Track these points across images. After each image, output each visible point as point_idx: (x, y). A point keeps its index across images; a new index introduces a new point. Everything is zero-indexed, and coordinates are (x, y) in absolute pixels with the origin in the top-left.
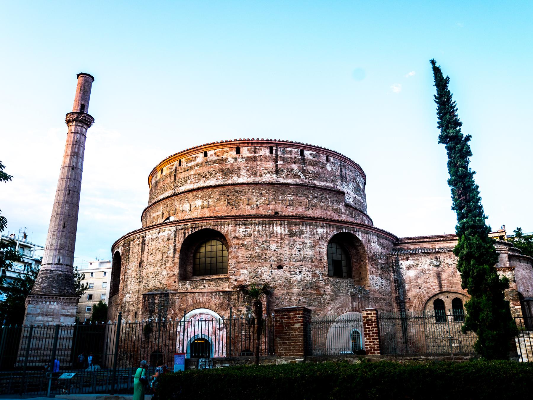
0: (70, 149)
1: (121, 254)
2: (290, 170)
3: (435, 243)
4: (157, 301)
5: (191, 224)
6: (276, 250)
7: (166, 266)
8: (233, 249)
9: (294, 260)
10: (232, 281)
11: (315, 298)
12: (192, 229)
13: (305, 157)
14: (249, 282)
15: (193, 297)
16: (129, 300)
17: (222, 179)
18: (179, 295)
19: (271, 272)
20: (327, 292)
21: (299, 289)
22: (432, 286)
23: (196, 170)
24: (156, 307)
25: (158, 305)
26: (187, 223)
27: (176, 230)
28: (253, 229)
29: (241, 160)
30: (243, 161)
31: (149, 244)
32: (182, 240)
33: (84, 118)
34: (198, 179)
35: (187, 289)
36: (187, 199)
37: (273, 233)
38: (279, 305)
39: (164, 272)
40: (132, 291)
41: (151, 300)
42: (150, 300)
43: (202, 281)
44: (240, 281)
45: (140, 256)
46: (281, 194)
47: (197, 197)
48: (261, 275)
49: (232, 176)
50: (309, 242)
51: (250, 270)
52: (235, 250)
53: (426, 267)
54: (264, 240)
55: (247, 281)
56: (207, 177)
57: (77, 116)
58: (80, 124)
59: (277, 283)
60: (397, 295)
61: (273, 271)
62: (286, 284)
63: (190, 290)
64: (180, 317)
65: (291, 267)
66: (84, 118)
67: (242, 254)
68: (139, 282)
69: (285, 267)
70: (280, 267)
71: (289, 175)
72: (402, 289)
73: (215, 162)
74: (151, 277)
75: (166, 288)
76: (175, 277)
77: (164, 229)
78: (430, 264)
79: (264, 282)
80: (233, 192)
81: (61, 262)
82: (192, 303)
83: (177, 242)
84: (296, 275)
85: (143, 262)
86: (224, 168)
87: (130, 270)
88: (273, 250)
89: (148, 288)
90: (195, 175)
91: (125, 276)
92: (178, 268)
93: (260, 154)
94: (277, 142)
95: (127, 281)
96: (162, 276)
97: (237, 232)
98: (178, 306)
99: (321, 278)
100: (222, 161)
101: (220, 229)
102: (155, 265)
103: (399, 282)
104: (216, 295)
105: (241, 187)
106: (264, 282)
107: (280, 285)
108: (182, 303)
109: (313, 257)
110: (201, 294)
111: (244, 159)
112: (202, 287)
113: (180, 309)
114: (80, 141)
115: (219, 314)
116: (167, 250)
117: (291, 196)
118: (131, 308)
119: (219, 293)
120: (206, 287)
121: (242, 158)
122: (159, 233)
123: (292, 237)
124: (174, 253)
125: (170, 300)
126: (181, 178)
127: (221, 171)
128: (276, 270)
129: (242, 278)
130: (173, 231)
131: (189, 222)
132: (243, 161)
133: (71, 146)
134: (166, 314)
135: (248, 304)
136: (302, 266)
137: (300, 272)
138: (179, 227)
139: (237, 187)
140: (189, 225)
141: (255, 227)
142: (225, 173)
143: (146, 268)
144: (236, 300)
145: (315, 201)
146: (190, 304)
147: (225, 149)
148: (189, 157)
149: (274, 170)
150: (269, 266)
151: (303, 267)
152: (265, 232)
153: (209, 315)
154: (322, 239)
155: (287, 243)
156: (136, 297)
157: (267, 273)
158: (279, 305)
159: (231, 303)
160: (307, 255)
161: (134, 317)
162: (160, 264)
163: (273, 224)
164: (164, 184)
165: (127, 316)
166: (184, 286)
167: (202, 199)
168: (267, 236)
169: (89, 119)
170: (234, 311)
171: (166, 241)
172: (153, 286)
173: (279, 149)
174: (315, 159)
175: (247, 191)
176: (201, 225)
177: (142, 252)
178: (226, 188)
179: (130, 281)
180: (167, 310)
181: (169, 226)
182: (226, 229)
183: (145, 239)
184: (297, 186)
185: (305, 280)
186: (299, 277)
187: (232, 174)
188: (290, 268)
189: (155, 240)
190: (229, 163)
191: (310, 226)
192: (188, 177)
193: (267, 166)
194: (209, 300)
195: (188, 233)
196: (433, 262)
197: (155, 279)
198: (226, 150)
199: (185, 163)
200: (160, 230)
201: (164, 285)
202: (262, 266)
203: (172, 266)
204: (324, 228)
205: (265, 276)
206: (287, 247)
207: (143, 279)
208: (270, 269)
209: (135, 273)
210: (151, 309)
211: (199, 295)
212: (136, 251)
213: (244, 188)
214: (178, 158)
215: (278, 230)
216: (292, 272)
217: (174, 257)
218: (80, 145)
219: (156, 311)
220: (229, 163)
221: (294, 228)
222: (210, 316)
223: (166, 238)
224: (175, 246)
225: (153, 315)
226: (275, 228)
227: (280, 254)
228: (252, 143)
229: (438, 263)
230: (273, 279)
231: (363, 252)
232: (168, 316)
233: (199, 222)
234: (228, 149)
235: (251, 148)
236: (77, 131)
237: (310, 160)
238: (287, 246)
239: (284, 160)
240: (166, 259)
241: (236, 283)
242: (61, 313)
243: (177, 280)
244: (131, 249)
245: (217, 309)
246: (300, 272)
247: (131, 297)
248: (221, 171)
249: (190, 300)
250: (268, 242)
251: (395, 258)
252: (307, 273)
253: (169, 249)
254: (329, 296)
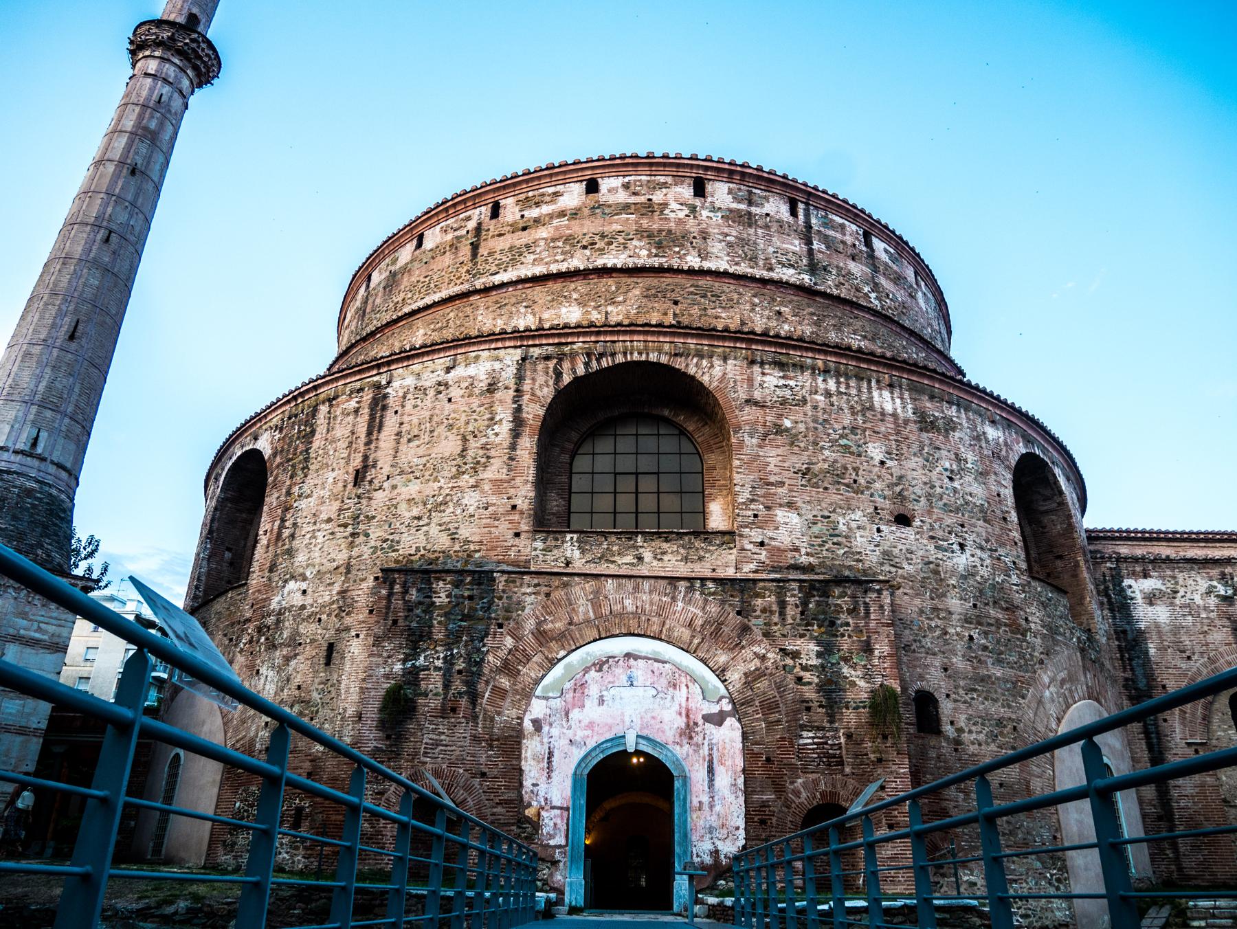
0: (134, 116)
1: (267, 453)
3: (1183, 544)
4: (441, 599)
5: (583, 342)
6: (888, 461)
7: (481, 476)
8: (747, 438)
9: (941, 503)
10: (750, 547)
11: (1009, 640)
12: (590, 360)
13: (877, 254)
14: (808, 554)
15: (597, 592)
16: (298, 600)
17: (649, 256)
18: (536, 581)
19: (879, 530)
20: (1033, 626)
21: (965, 600)
22: (1220, 653)
23: (557, 228)
24: (437, 618)
25: (446, 615)
26: (569, 340)
27: (524, 359)
28: (808, 384)
29: (711, 215)
31: (403, 406)
32: (547, 393)
33: (194, 45)
34: (563, 253)
35: (568, 564)
36: (524, 304)
37: (872, 408)
38: (914, 647)
39: (471, 500)
40: (317, 568)
41: (419, 590)
42: (414, 591)
43: (630, 539)
44: (779, 549)
45: (362, 448)
46: (835, 326)
47: (565, 297)
48: (850, 537)
49: (682, 252)
50: (970, 457)
51: (810, 517)
52: (754, 441)
53: (1198, 600)
54: (847, 422)
55: (803, 551)
56: (597, 246)
57: (173, 34)
58: (176, 61)
59: (900, 571)
60: (1129, 674)
61: (883, 527)
62: (928, 578)
63: (578, 565)
64: (541, 666)
65: (936, 526)
66: (194, 45)
67: (780, 458)
68: (353, 535)
69: (917, 523)
70: (903, 520)
71: (843, 284)
72: (1138, 657)
73: (626, 208)
74: (408, 515)
75: (477, 555)
76: (516, 517)
77: (473, 354)
78: (1209, 593)
79: (858, 561)
80: (692, 293)
81: (39, 450)
82: (591, 615)
83: (526, 397)
84: (953, 552)
85: (374, 466)
86: (654, 226)
87: (309, 499)
88: (876, 462)
89: (393, 554)
90: (553, 240)
91: (283, 520)
92: (529, 487)
93: (765, 210)
94: (809, 189)
95: (292, 536)
96: (458, 512)
97: (756, 384)
98: (532, 621)
99: (1013, 577)
100: (649, 208)
101: (694, 369)
102: (427, 474)
103: (1130, 637)
104: (691, 589)
105: (717, 285)
106: (858, 561)
107: (910, 578)
108: (550, 614)
109: (986, 505)
110: (629, 584)
111: (719, 214)
112: (629, 559)
113: (542, 636)
114: (168, 105)
115: (704, 661)
116: (486, 423)
117: (860, 341)
118: (308, 629)
119: (703, 585)
120: (646, 560)
121: (714, 209)
122: (448, 370)
123: (928, 432)
124: (516, 434)
125: (500, 598)
126: (498, 249)
127: (645, 234)
128: (894, 528)
129: (783, 538)
130: (510, 363)
131: (579, 334)
132: (714, 219)
133: (137, 109)
134: (479, 650)
135: (823, 630)
136: (962, 526)
137: (962, 546)
138: (536, 352)
139: (703, 282)
140: (579, 344)
141: (815, 380)
142: (660, 242)
143: (386, 485)
144: (772, 612)
146: (581, 617)
147: (658, 177)
148: (530, 194)
149: (805, 261)
150: (871, 510)
151: (966, 532)
152: (848, 401)
153: (665, 662)
154: (999, 458)
155: (915, 448)
156: (336, 588)
157: (867, 533)
158: (914, 647)
159: (754, 621)
160: (971, 494)
161: (322, 661)
162: (454, 470)
163: (869, 382)
164: (430, 273)
165: (288, 659)
166: (555, 551)
167: (580, 303)
168: (853, 414)
169: (207, 55)
170: (768, 651)
171: (481, 394)
172: (418, 549)
173: (813, 212)
174: (895, 267)
175: (736, 296)
176: (626, 348)
177: (369, 433)
178: (667, 280)
179: (308, 536)
180: (487, 635)
181: (493, 346)
182: (717, 371)
183: (388, 390)
184: (873, 315)
185: (977, 573)
186: (962, 561)
187: (682, 246)
188: (932, 528)
189: (432, 393)
190: (672, 215)
191: (966, 410)
192: (528, 246)
193: (784, 246)
194: (661, 608)
195: (573, 370)
196: (1216, 587)
197: (428, 524)
198: (662, 181)
199: (518, 208)
200: (455, 360)
201: (467, 542)
202: (849, 508)
203: (504, 477)
204: (998, 429)
205: (860, 541)
206: (917, 459)
207: (374, 522)
208: (873, 522)
209: (336, 505)
210: (414, 624)
211: (619, 586)
212: (341, 431)
213: (725, 288)
214: (490, 198)
215: (885, 400)
216: (941, 543)
217: (513, 447)
218: (168, 116)
219: (438, 633)
220: (672, 215)
221: (928, 405)
222: (667, 666)
223: (483, 385)
224: (518, 410)
225: (424, 651)
226: (875, 394)
227: (900, 478)
228: (743, 174)
229: (1230, 592)
230: (887, 555)
231: (1066, 529)
232: (490, 658)
233: (615, 338)
234: (669, 180)
235: (739, 189)
236: (163, 76)
237: (886, 264)
238: (915, 455)
239: (826, 239)
240: (481, 452)
241: (764, 553)
242: (12, 631)
243: (524, 527)
244: (321, 430)
245: (696, 641)
246: (962, 546)
247: (309, 591)
249: (581, 602)
250: (859, 432)
251: (1111, 568)
252: (978, 552)
253: (492, 419)
254: (1039, 641)
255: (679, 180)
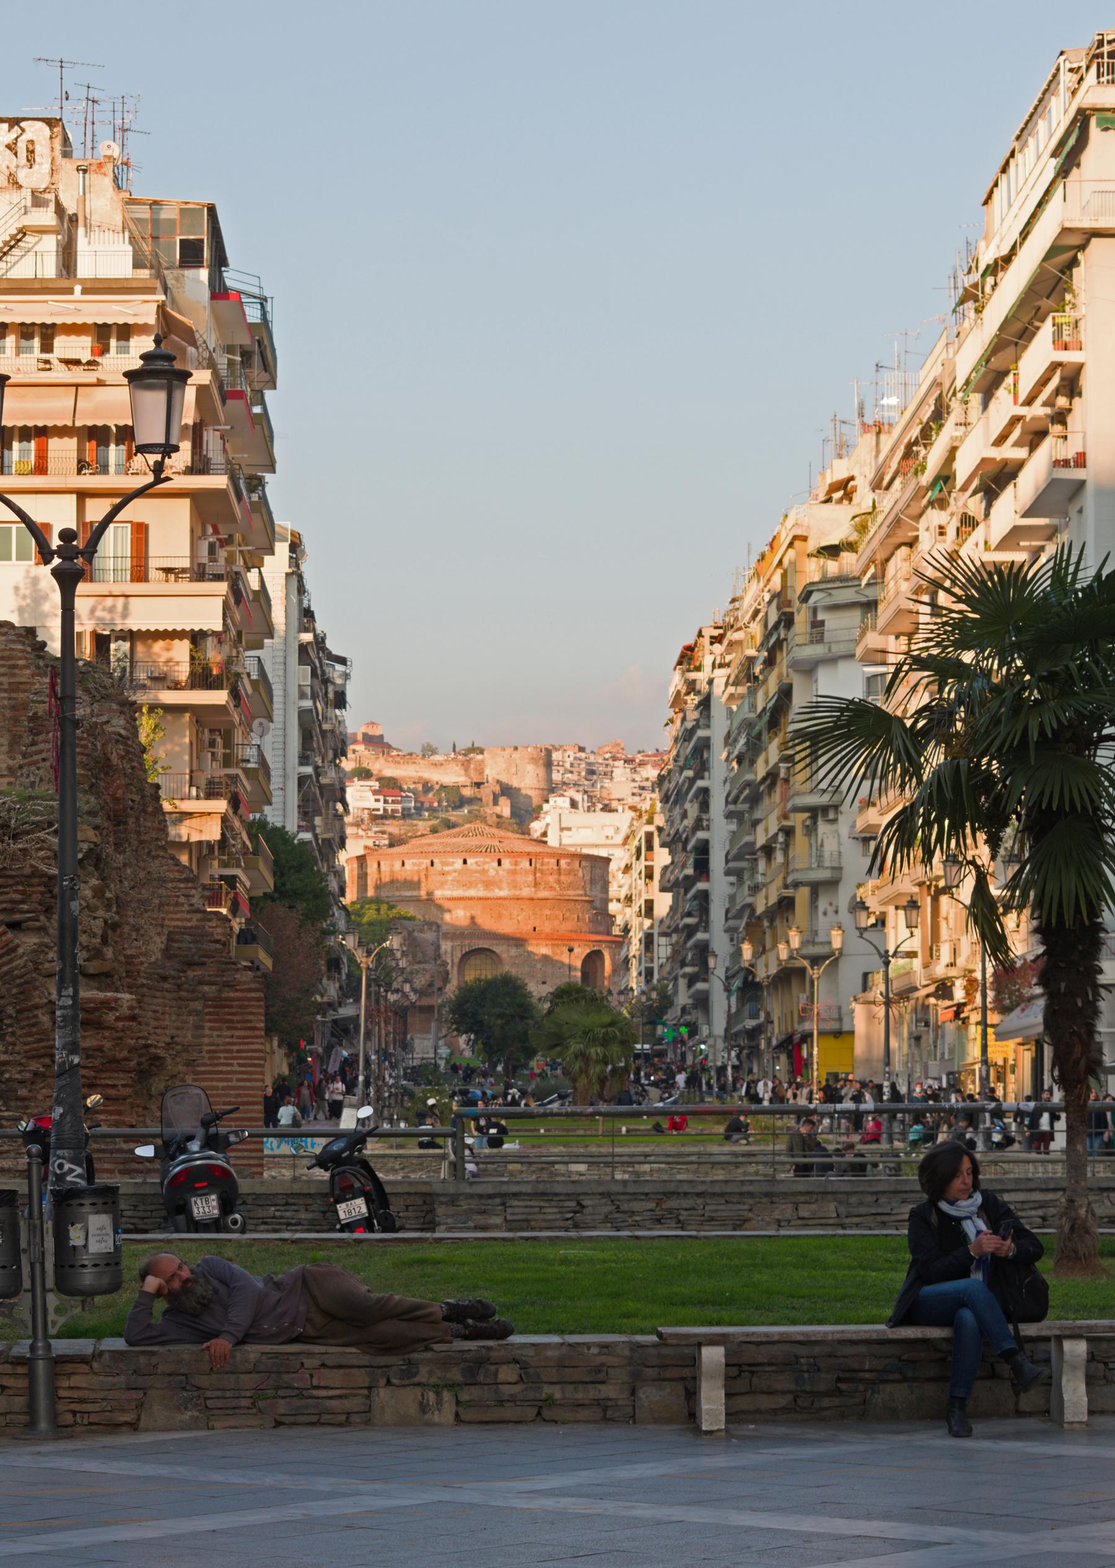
2: (547, 883)
30: (505, 874)
32: (459, 956)
70: (544, 983)
73: (476, 872)
105: (504, 902)
145: (568, 914)
167: (464, 909)
239: (542, 871)
248: (483, 882)
255: (493, 861)
